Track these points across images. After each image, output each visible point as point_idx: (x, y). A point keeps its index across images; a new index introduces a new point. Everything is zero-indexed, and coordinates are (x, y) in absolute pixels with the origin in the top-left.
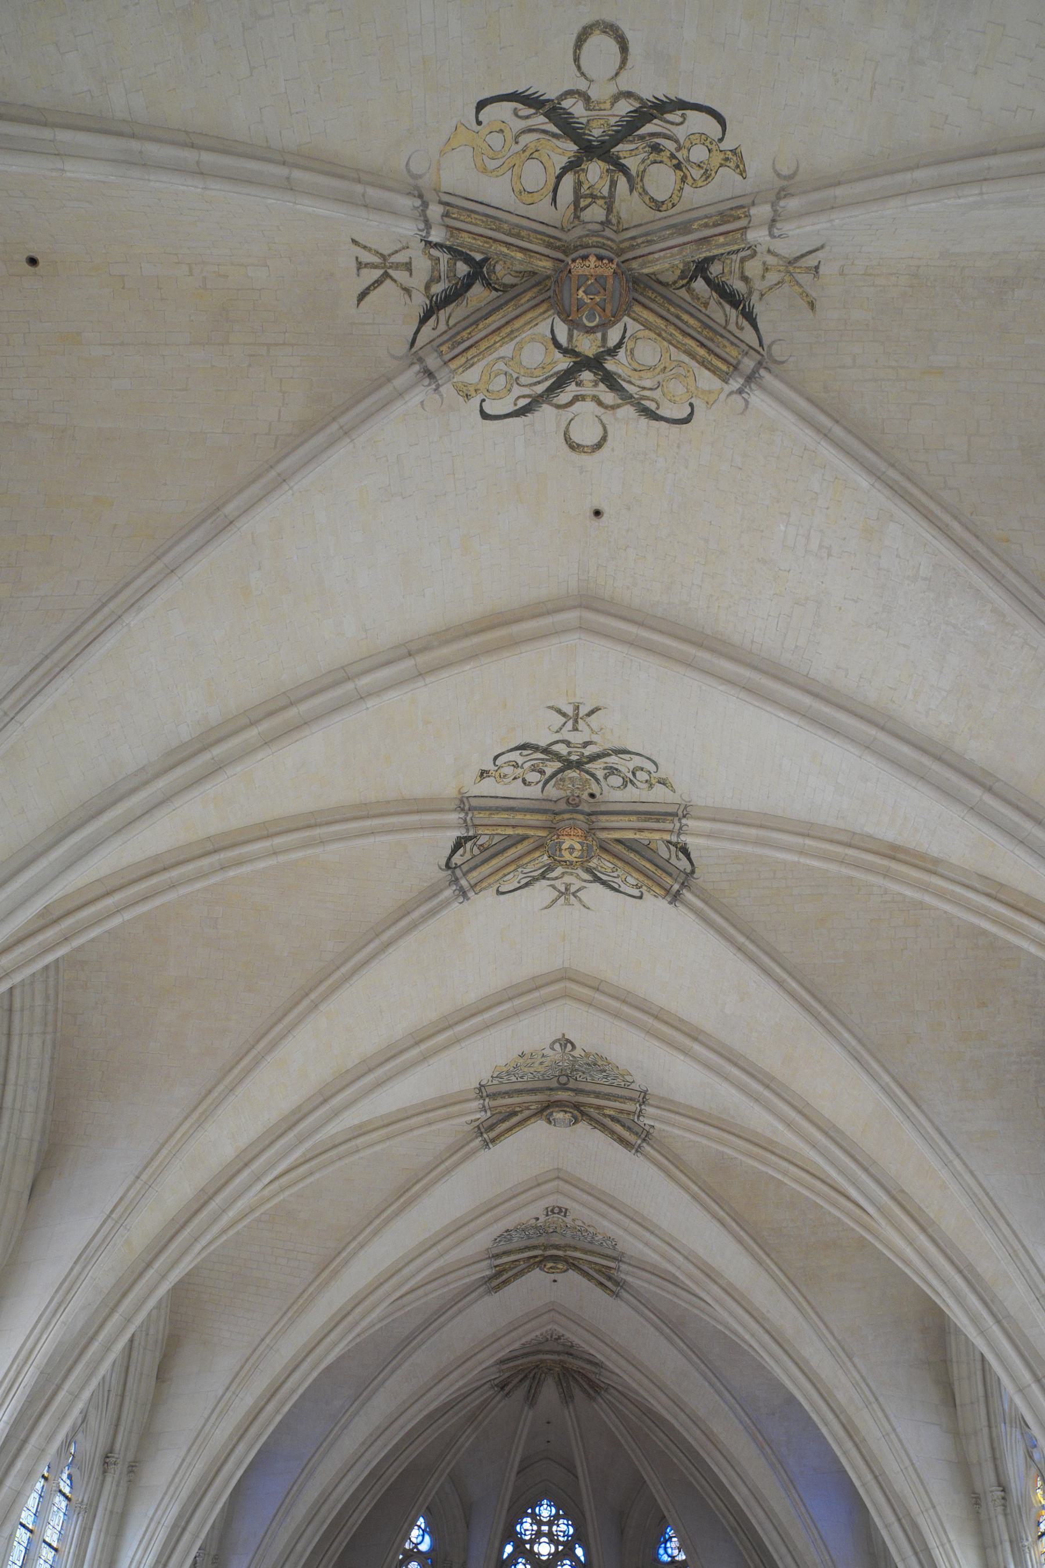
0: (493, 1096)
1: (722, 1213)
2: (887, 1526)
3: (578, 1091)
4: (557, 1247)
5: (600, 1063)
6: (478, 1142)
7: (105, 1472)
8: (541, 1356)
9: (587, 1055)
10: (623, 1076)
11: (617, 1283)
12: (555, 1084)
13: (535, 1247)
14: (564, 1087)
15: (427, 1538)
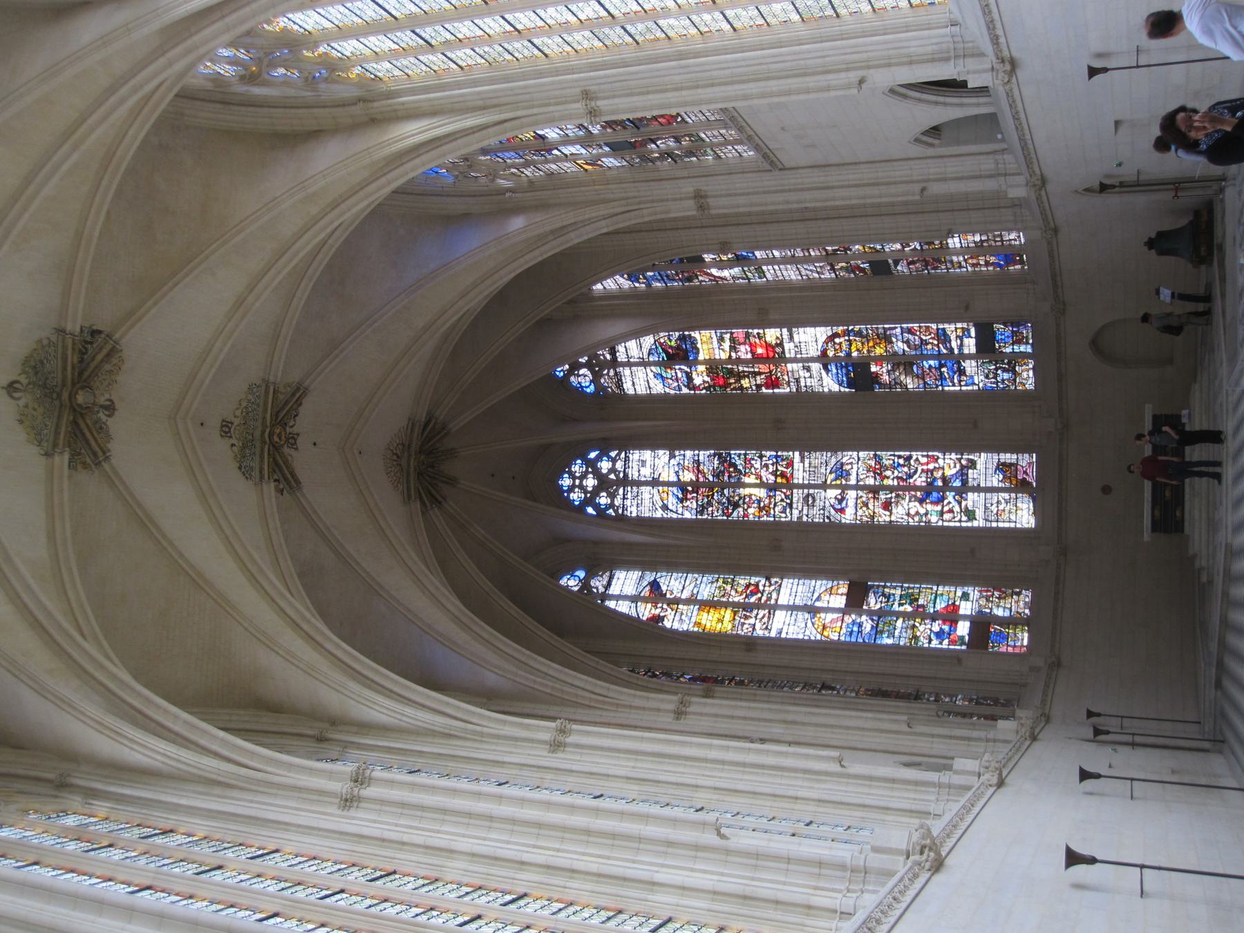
0: (55, 445)
1: (170, 284)
2: (389, 183)
3: (64, 385)
4: (263, 432)
5: (32, 363)
6: (106, 465)
7: (327, 740)
8: (412, 470)
9: (24, 372)
10: (43, 347)
11: (298, 389)
12: (57, 403)
13: (262, 450)
14: (59, 395)
15: (577, 573)
